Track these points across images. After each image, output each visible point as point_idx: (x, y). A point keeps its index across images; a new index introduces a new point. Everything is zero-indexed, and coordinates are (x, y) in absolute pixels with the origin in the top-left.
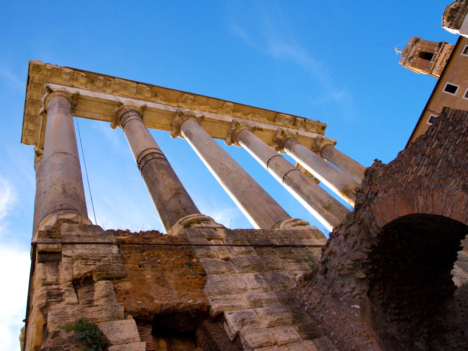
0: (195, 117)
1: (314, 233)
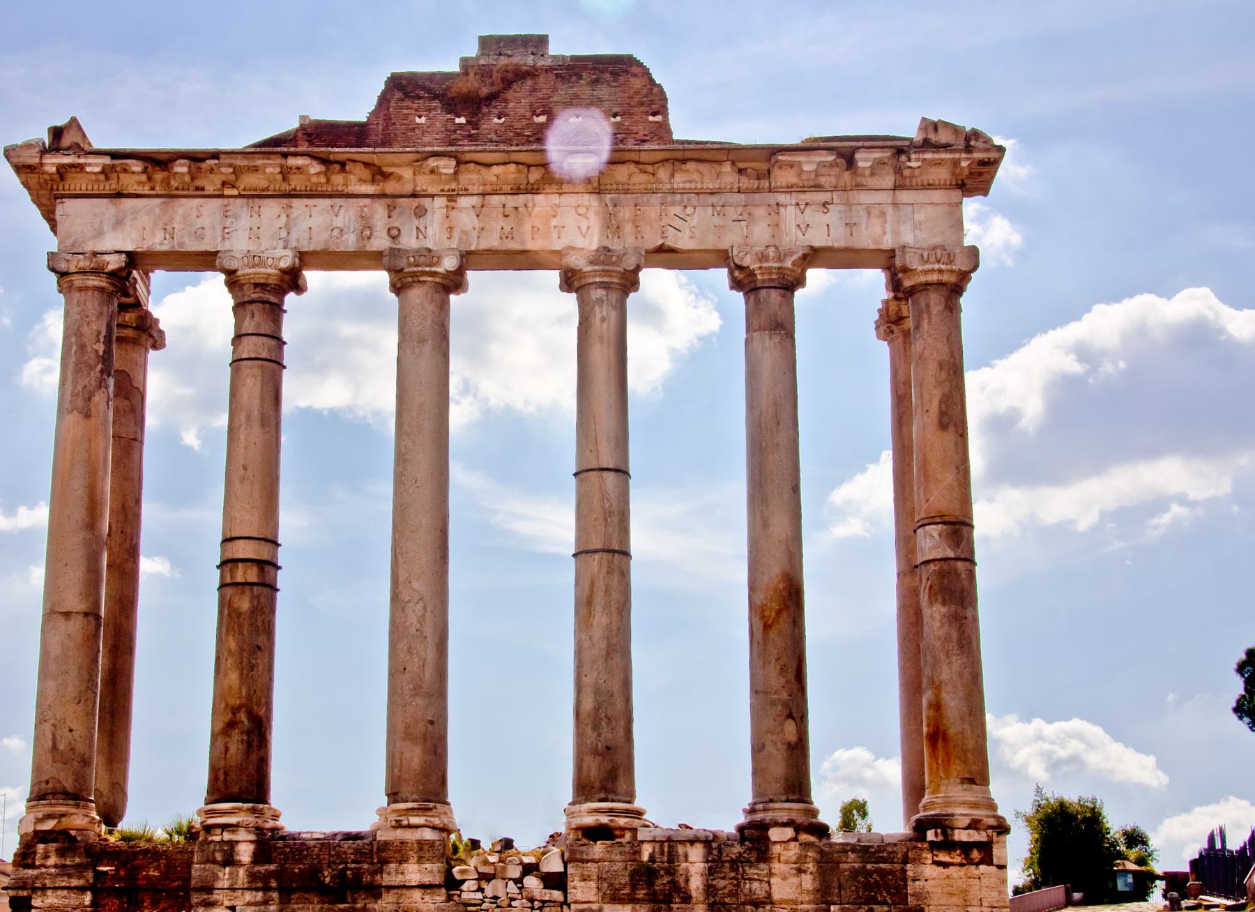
0: (434, 274)
1: (421, 849)
